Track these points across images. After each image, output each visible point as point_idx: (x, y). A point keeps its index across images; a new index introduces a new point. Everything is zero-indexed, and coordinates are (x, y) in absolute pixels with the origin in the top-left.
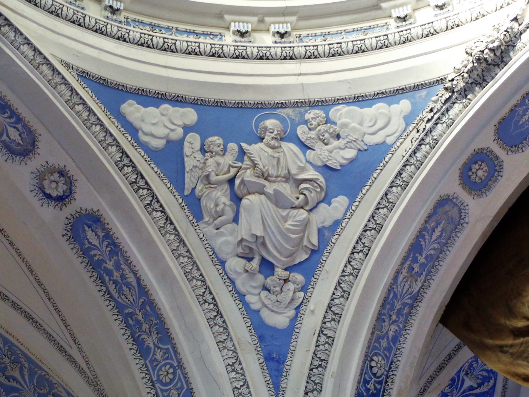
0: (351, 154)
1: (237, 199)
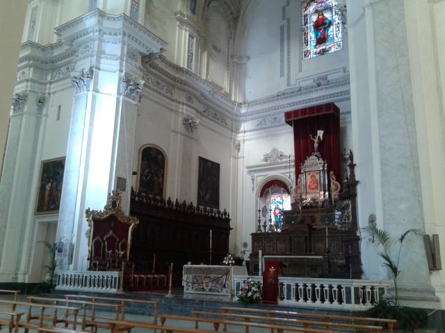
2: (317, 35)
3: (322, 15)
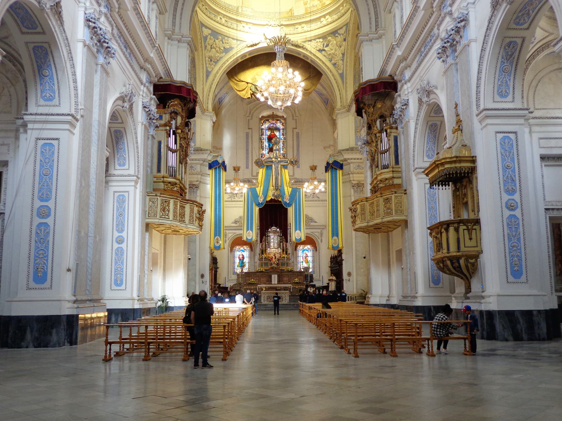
0: (228, 47)
1: (211, 48)
2: (269, 145)
3: (274, 132)
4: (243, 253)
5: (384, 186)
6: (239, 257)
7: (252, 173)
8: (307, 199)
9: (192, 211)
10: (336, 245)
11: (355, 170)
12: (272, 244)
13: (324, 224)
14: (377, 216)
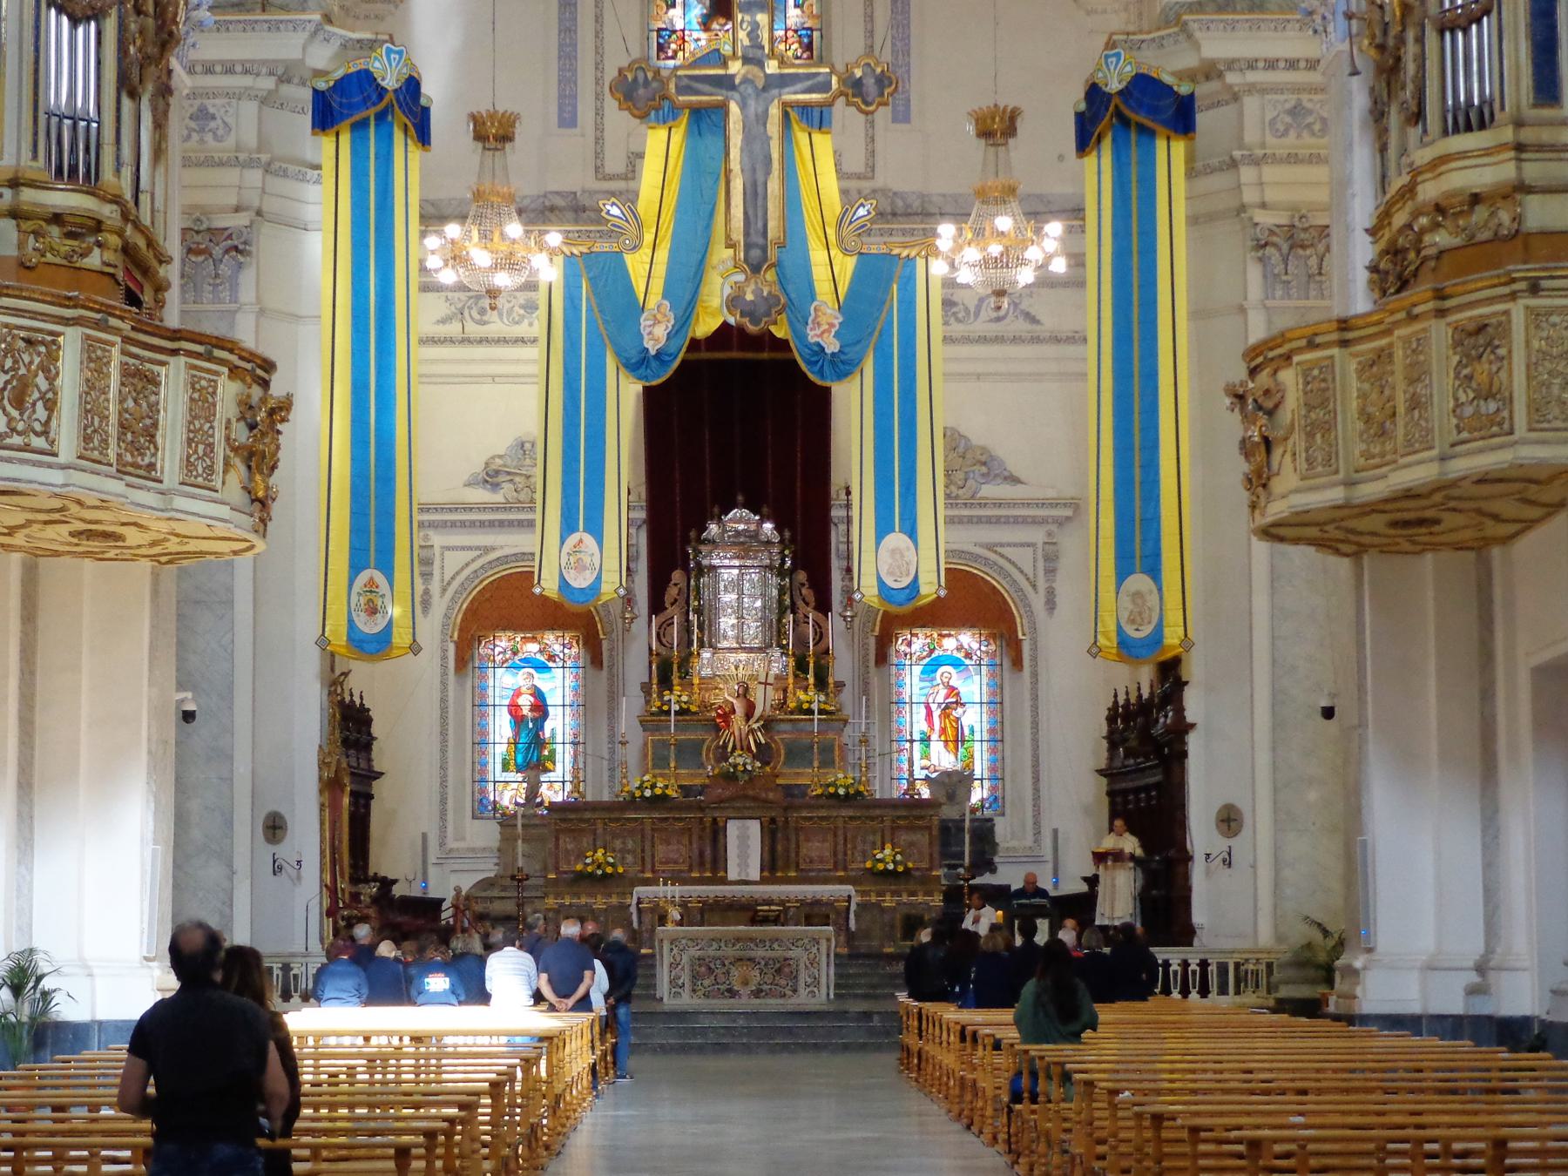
4: (544, 682)
5: (1457, 241)
6: (514, 709)
7: (599, 155)
8: (957, 329)
9: (201, 404)
10: (1147, 630)
11: (1270, 140)
12: (727, 623)
13: (1069, 492)
14: (1409, 443)
